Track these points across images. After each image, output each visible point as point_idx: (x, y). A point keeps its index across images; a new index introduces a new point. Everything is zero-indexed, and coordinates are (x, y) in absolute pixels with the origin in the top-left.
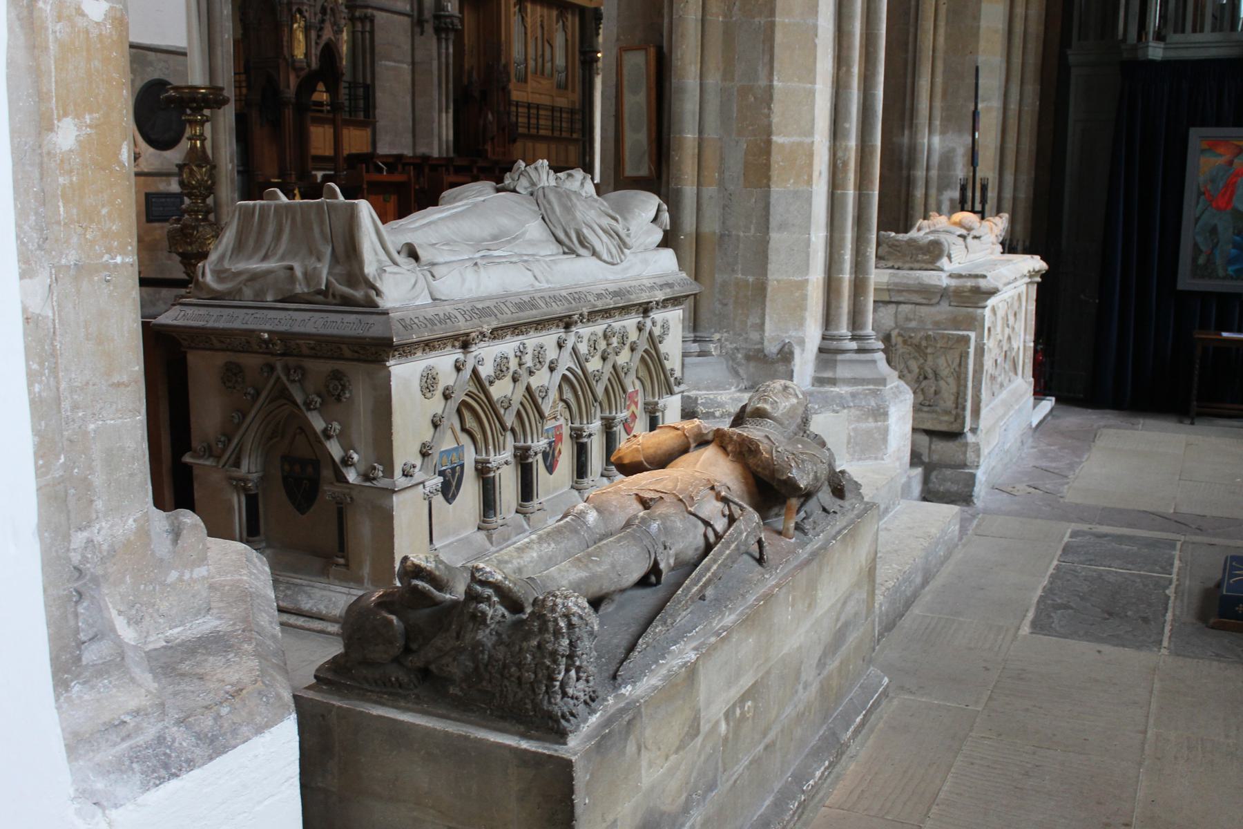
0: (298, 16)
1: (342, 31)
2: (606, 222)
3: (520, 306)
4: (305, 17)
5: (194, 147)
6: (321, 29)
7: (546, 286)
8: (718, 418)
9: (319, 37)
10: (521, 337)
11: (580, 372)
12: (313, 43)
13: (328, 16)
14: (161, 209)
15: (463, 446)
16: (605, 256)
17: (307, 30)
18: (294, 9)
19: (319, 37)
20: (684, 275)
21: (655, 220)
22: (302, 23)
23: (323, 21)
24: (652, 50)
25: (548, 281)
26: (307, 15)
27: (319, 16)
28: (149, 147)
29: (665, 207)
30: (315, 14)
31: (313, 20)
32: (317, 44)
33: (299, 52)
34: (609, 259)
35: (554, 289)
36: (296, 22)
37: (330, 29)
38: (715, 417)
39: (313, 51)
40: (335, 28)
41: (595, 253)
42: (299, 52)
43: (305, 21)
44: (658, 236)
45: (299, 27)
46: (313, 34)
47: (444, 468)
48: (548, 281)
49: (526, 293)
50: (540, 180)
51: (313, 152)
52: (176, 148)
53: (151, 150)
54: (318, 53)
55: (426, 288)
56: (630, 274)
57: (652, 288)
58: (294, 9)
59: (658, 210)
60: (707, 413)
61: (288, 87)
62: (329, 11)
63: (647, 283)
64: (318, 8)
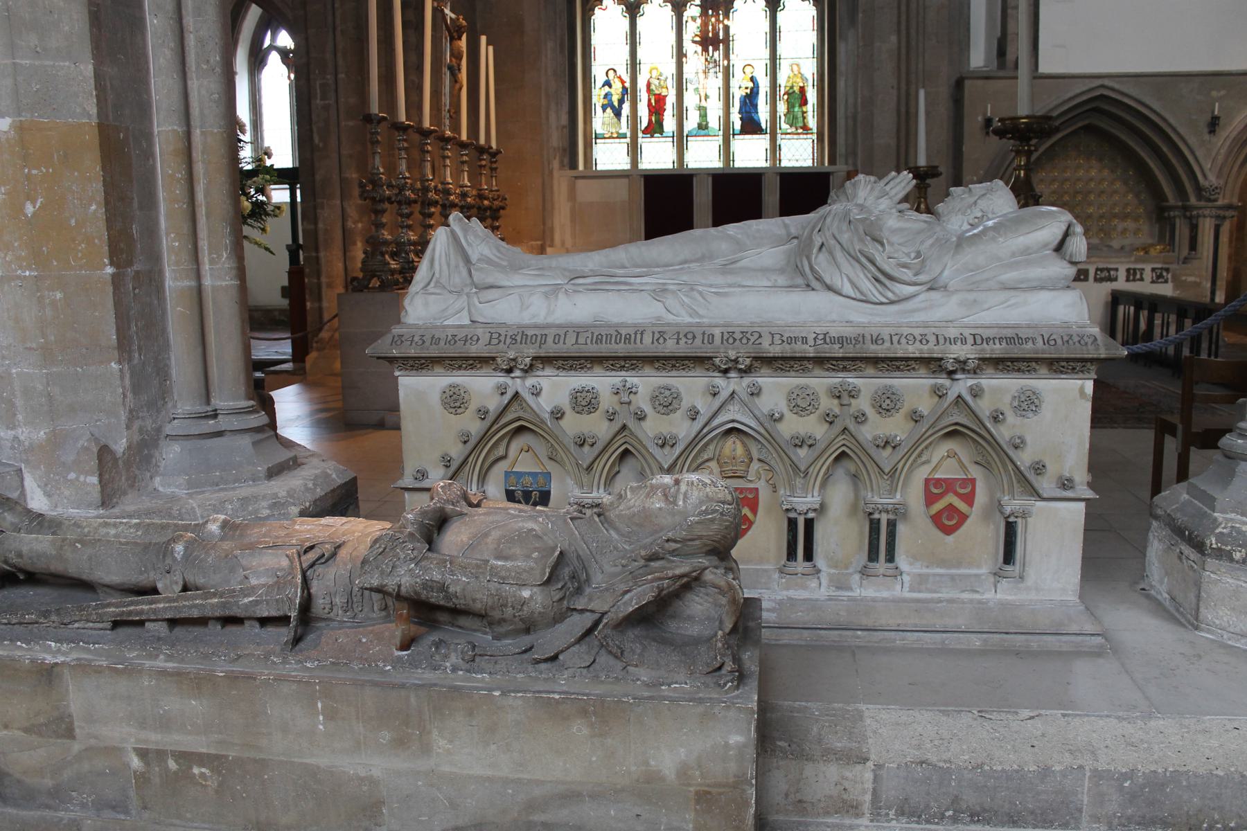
2: (857, 247)
3: (599, 339)
5: (1018, 177)
7: (688, 319)
8: (1237, 562)
10: (623, 373)
11: (762, 431)
15: (550, 473)
16: (848, 289)
21: (1059, 248)
25: (693, 313)
29: (1079, 229)
34: (859, 296)
35: (699, 325)
38: (1232, 560)
41: (829, 288)
47: (511, 488)
48: (693, 313)
49: (635, 325)
55: (466, 308)
59: (1066, 235)
60: (1219, 549)
63: (952, 333)
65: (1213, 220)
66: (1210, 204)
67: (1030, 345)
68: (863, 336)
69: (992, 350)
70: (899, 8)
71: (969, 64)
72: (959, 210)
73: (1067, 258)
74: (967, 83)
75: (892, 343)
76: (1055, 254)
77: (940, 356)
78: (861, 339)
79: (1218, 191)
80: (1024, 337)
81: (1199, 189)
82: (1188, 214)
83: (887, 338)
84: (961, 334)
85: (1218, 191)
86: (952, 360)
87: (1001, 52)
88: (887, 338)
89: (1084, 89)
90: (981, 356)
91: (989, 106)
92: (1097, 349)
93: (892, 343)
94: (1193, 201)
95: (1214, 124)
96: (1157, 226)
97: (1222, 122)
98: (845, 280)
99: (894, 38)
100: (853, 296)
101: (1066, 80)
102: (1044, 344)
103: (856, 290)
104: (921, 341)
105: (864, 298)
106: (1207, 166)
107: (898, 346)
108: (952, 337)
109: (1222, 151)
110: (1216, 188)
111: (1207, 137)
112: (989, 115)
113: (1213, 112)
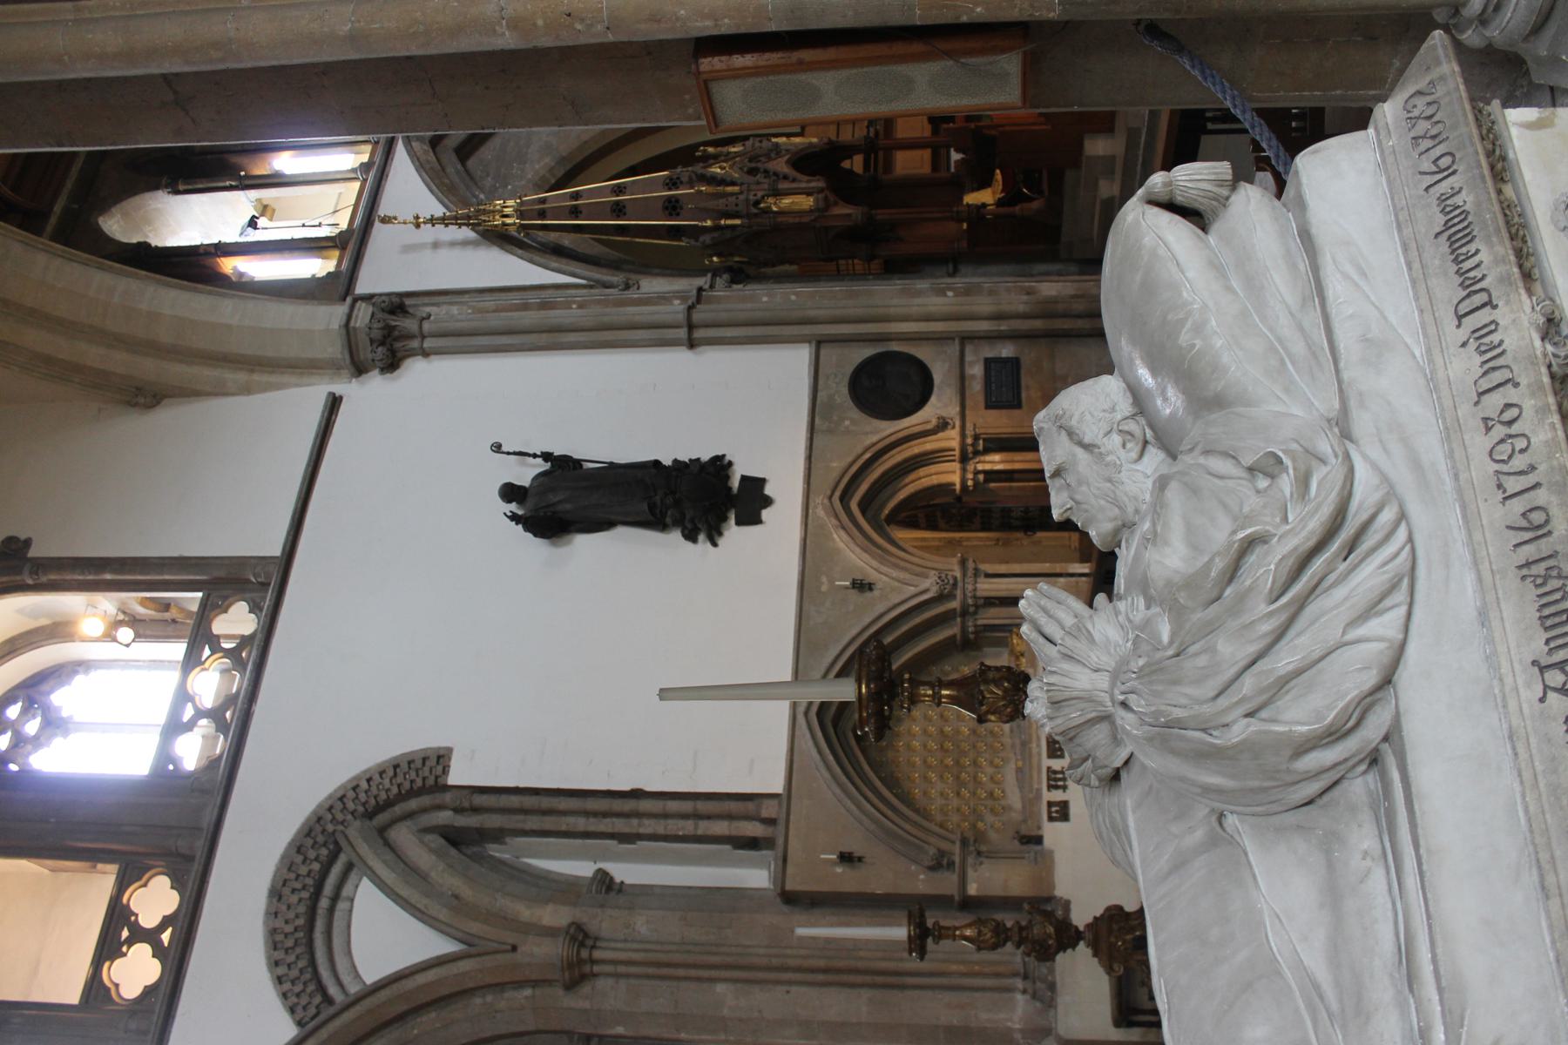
0: (762, 205)
1: (777, 144)
2: (1264, 608)
4: (763, 197)
5: (954, 700)
6: (776, 174)
9: (785, 177)
12: (794, 185)
13: (759, 165)
14: (1004, 389)
17: (778, 194)
18: (754, 211)
19: (785, 177)
20: (1388, 112)
22: (771, 200)
23: (766, 172)
24: (710, 64)
26: (760, 194)
27: (759, 177)
28: (929, 403)
29: (1157, 179)
30: (758, 183)
31: (766, 186)
32: (794, 180)
33: (806, 202)
34: (1401, 596)
36: (770, 207)
37: (775, 162)
39: (803, 185)
40: (773, 155)
42: (806, 202)
43: (768, 196)
44: (1251, 201)
45: (775, 204)
46: (783, 185)
50: (1090, 700)
51: (926, 169)
52: (929, 366)
53: (933, 399)
54: (806, 178)
56: (1432, 449)
57: (1485, 342)
58: (755, 211)
59: (1171, 207)
61: (849, 215)
62: (753, 165)
63: (1464, 366)
64: (750, 179)
65: (979, 580)
66: (960, 584)
67: (1466, 199)
68: (1528, 564)
69: (1498, 261)
70: (678, 978)
71: (765, 889)
72: (1110, 480)
73: (1225, 192)
74: (788, 887)
75: (1537, 486)
76: (1216, 228)
77: (1544, 370)
78: (1539, 569)
79: (943, 576)
80: (1441, 219)
81: (941, 598)
82: (972, 609)
83: (1518, 506)
84: (1464, 345)
85: (943, 576)
86: (1550, 348)
87: (752, 844)
88: (1518, 506)
89: (808, 735)
90: (1520, 284)
91: (822, 856)
92: (1442, 78)
93: (1537, 486)
94: (955, 604)
95: (862, 586)
96: (985, 649)
97: (859, 577)
98: (1361, 631)
99: (720, 988)
100: (1403, 610)
101: (796, 758)
102: (1454, 172)
103: (1388, 602)
104: (1510, 423)
105: (1406, 581)
106: (912, 590)
107: (1542, 468)
108: (1478, 359)
109: (895, 573)
110: (939, 578)
111: (876, 593)
112: (835, 857)
113: (846, 588)
